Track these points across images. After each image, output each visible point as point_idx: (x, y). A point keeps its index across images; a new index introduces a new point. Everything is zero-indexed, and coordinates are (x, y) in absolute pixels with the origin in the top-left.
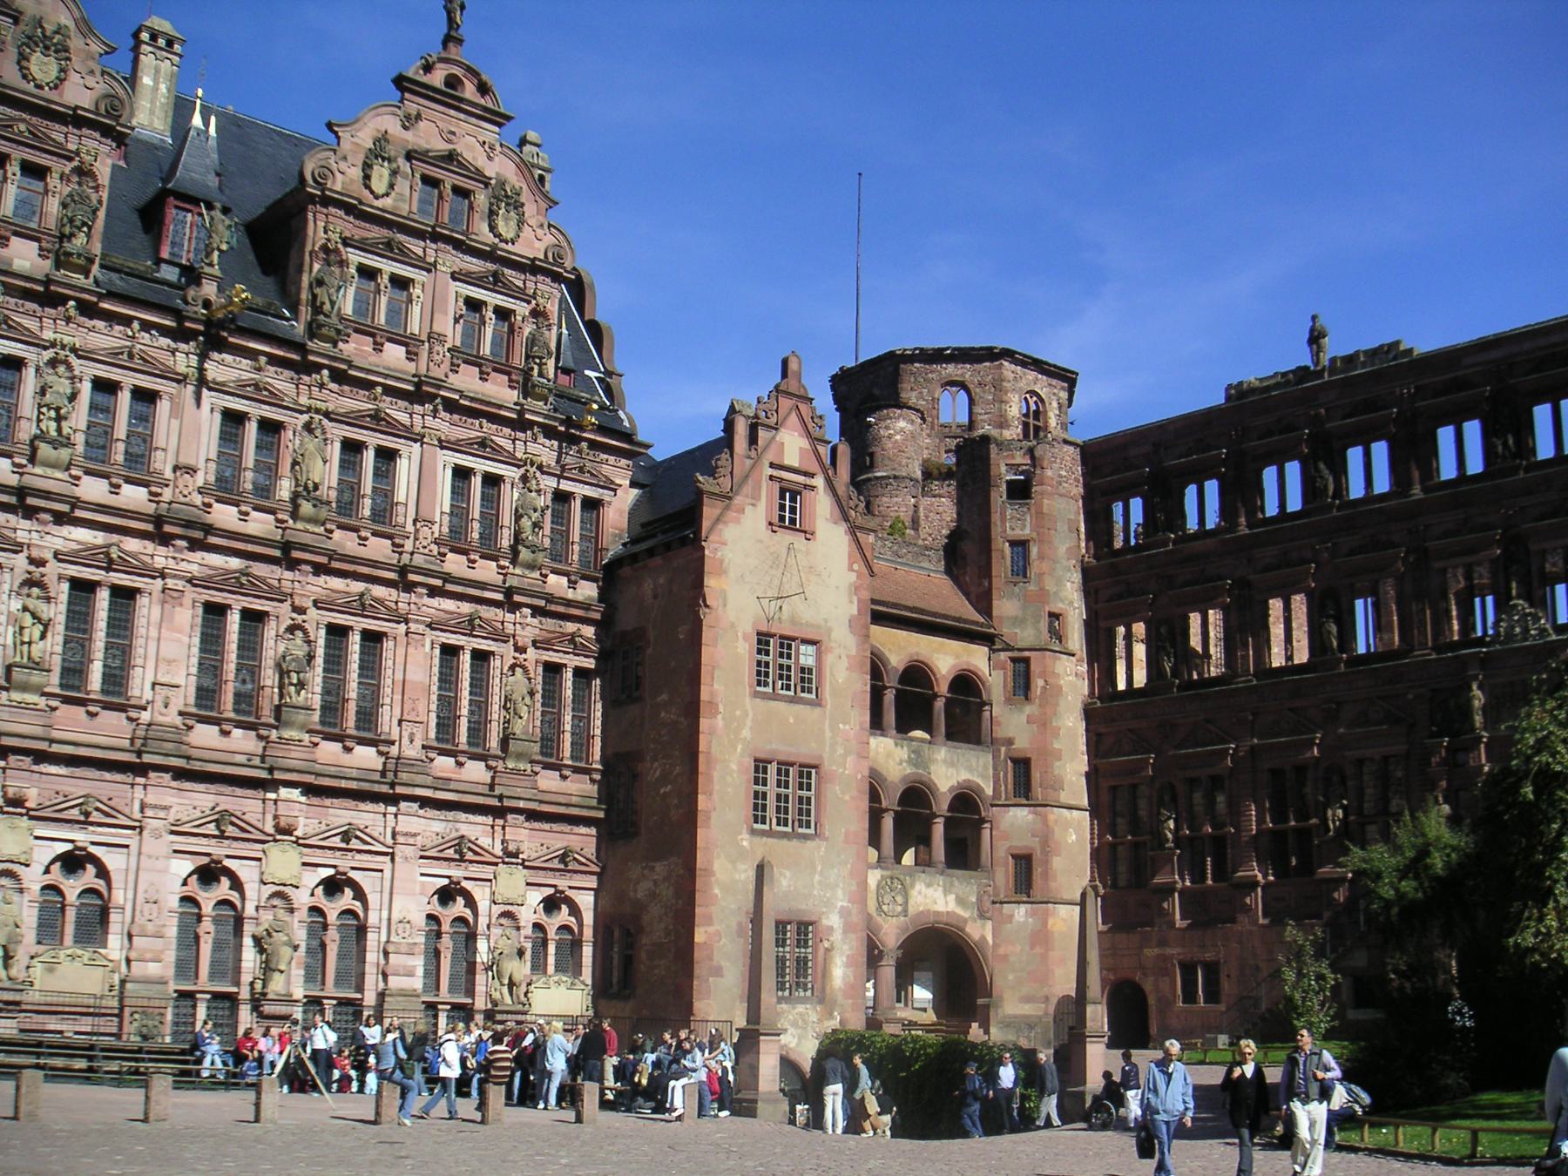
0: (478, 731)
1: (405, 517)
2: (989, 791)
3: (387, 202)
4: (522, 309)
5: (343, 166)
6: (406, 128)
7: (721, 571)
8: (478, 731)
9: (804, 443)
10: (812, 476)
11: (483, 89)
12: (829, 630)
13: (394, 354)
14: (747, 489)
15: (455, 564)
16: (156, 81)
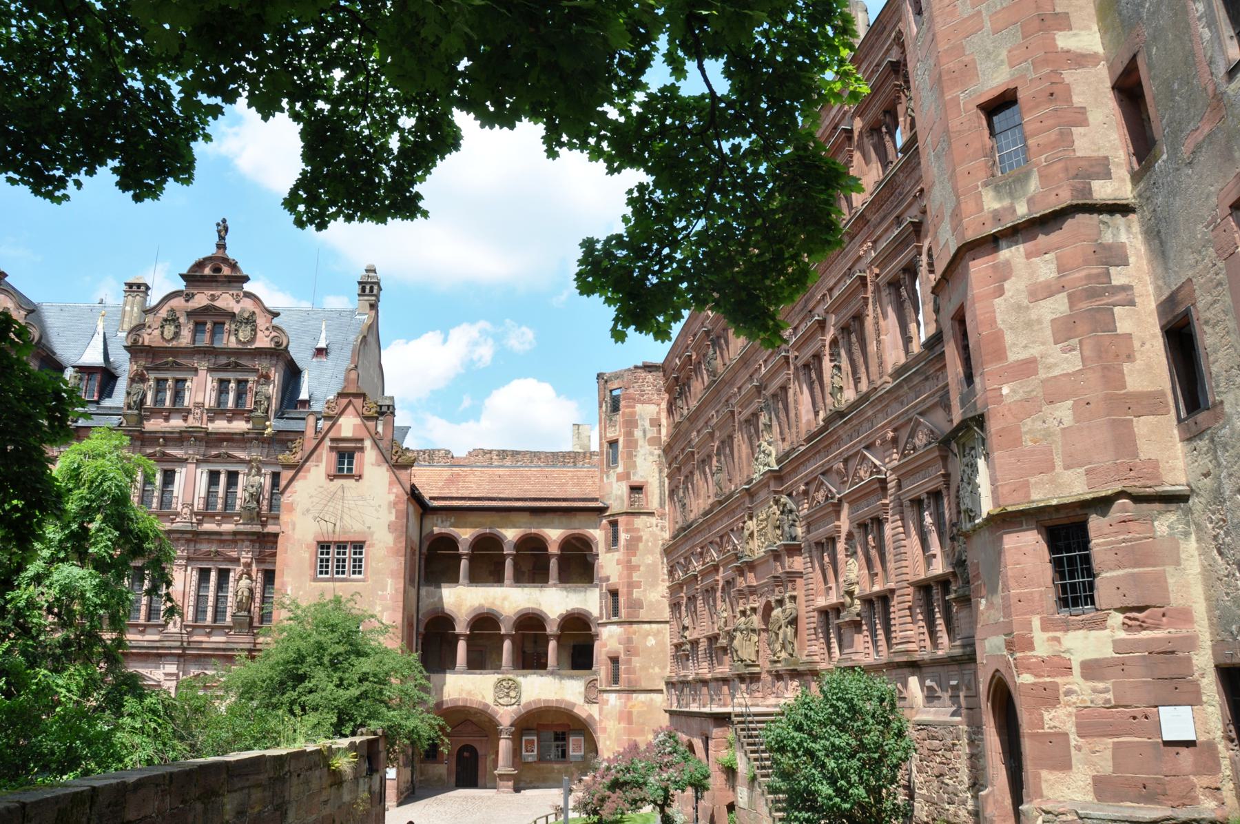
0: (218, 613)
1: (178, 506)
2: (595, 612)
3: (174, 343)
4: (252, 378)
5: (149, 331)
6: (187, 301)
7: (291, 508)
8: (218, 613)
9: (358, 421)
10: (362, 440)
11: (234, 266)
12: (372, 534)
13: (176, 423)
14: (314, 457)
15: (208, 526)
16: (132, 308)
